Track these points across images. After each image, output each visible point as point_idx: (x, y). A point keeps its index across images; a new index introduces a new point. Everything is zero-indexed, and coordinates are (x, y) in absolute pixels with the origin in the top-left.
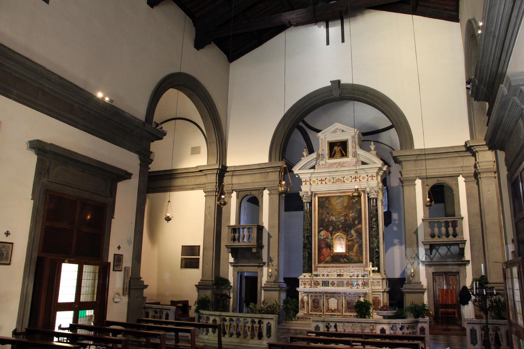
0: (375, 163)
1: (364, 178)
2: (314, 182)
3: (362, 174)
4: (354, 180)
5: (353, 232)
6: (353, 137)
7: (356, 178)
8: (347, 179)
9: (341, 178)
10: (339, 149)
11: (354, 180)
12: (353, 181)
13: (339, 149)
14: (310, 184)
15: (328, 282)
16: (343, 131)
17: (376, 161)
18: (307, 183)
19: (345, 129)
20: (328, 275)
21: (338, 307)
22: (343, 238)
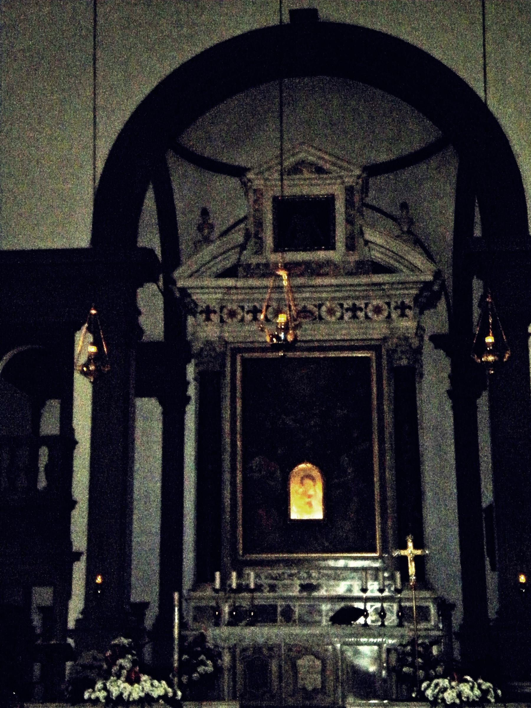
0: (413, 268)
1: (378, 310)
2: (232, 314)
3: (375, 298)
4: (350, 314)
5: (345, 459)
6: (349, 190)
7: (354, 309)
8: (331, 312)
9: (310, 307)
10: (303, 223)
11: (350, 314)
12: (346, 318)
13: (303, 223)
14: (222, 321)
15: (275, 607)
16: (320, 170)
17: (419, 264)
18: (212, 316)
19: (327, 166)
20: (273, 588)
21: (323, 682)
22: (313, 479)
